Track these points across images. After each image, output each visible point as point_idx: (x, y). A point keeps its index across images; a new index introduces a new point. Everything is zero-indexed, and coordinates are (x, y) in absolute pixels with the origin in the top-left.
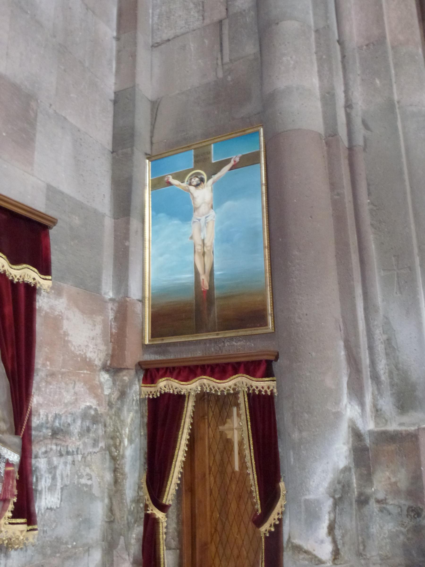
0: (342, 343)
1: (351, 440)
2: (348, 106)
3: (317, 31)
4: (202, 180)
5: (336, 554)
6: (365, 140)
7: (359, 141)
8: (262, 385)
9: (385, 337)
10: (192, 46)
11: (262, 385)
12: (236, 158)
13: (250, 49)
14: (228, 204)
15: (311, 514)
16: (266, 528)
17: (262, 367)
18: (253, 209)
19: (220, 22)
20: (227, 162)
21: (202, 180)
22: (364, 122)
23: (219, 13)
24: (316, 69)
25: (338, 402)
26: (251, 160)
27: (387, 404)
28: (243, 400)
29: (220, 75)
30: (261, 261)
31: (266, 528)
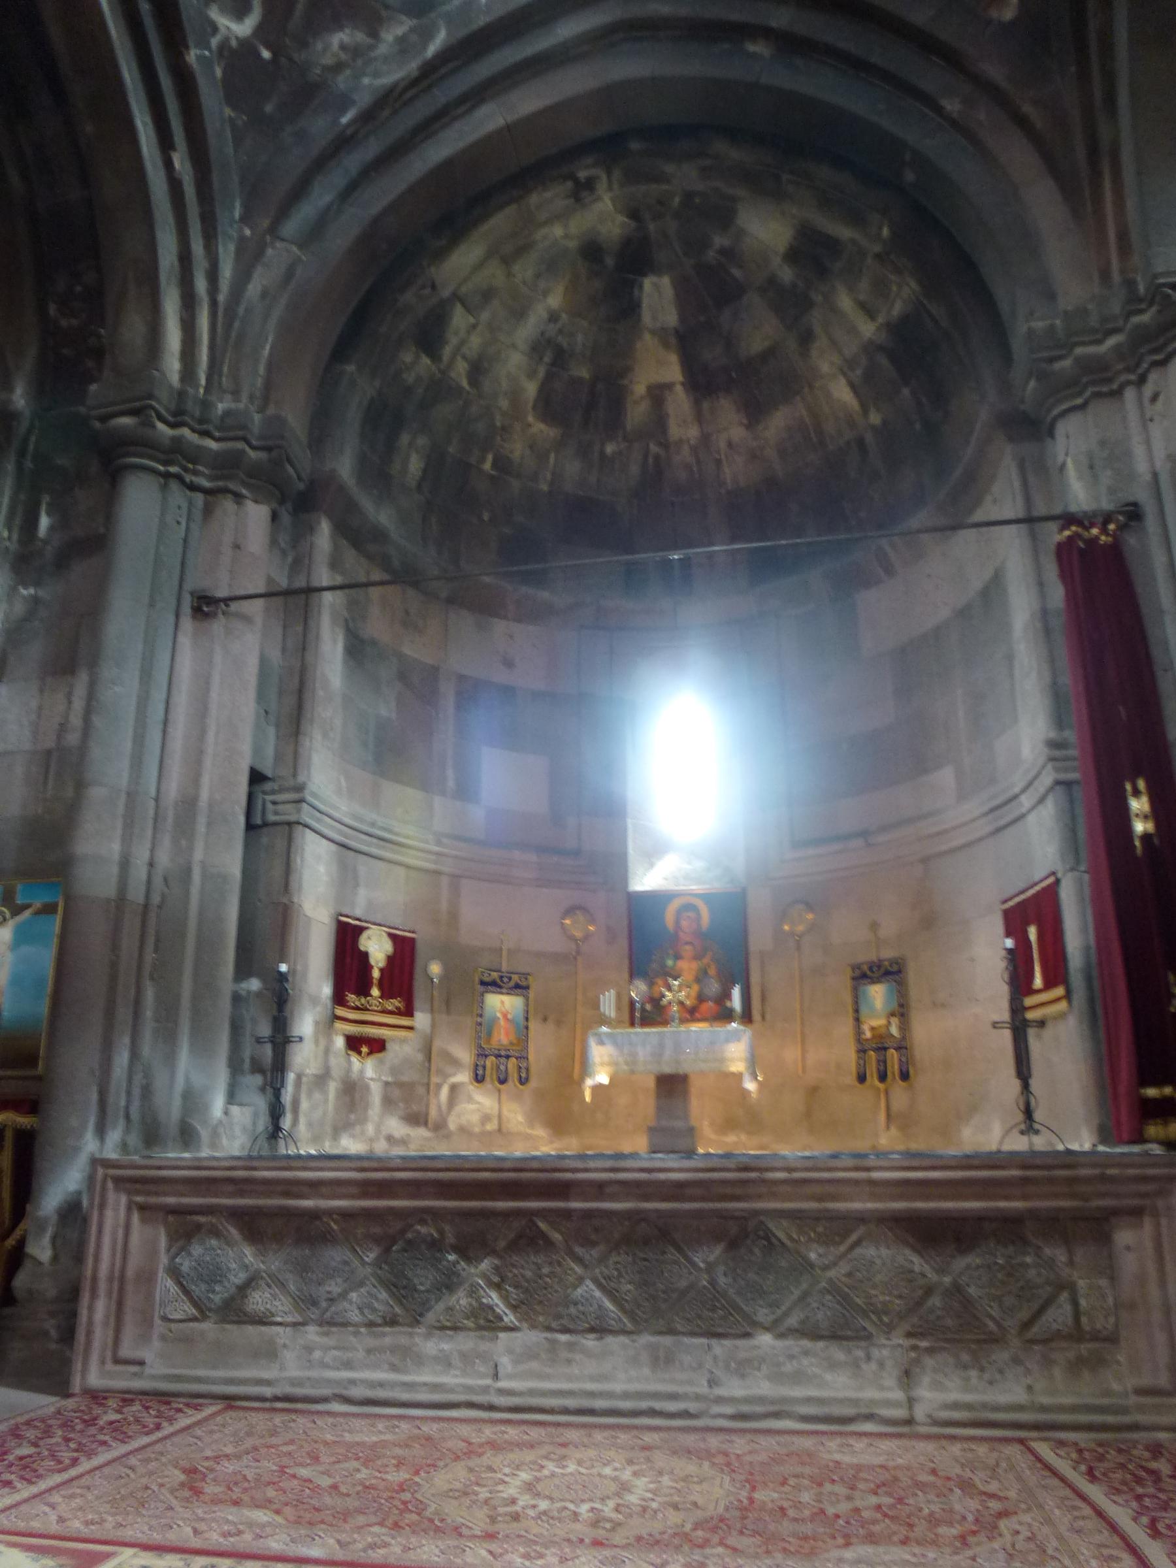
0: (95, 1089)
1: (88, 1169)
2: (151, 865)
3: (128, 794)
4: (5, 919)
5: (55, 1258)
6: (163, 896)
7: (156, 899)
8: (24, 1121)
9: (144, 1082)
10: (19, 770)
11: (24, 1121)
12: (38, 904)
13: (69, 792)
14: (26, 949)
15: (41, 1227)
16: (10, 1242)
17: (32, 1106)
18: (45, 957)
19: (49, 753)
20: (27, 906)
21: (5, 919)
22: (166, 880)
23: (50, 743)
24: (119, 832)
25: (80, 1136)
26: (49, 909)
27: (134, 1140)
28: (9, 1135)
29: (40, 811)
30: (44, 1008)
31: (10, 1242)
